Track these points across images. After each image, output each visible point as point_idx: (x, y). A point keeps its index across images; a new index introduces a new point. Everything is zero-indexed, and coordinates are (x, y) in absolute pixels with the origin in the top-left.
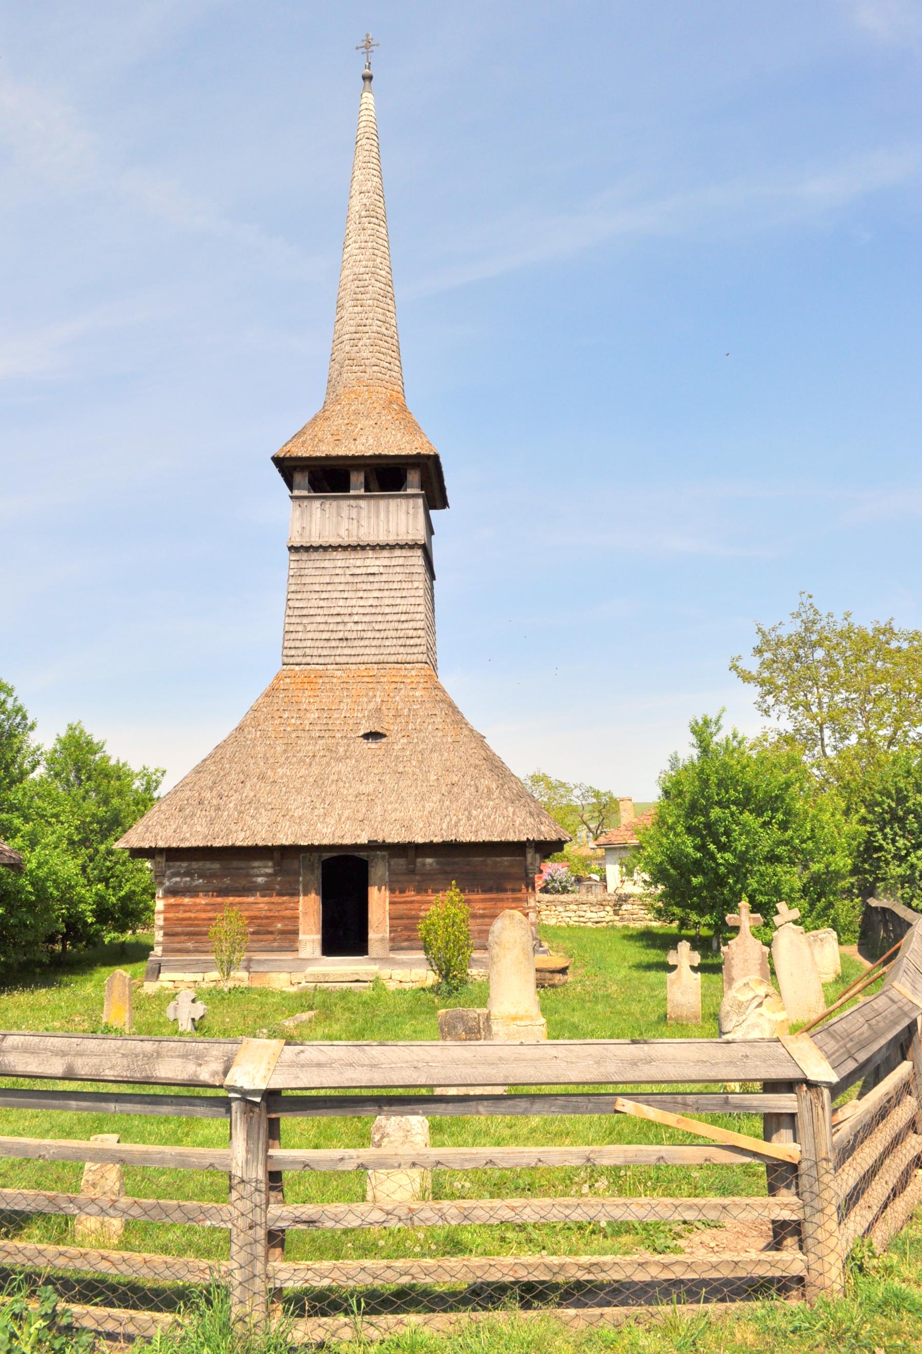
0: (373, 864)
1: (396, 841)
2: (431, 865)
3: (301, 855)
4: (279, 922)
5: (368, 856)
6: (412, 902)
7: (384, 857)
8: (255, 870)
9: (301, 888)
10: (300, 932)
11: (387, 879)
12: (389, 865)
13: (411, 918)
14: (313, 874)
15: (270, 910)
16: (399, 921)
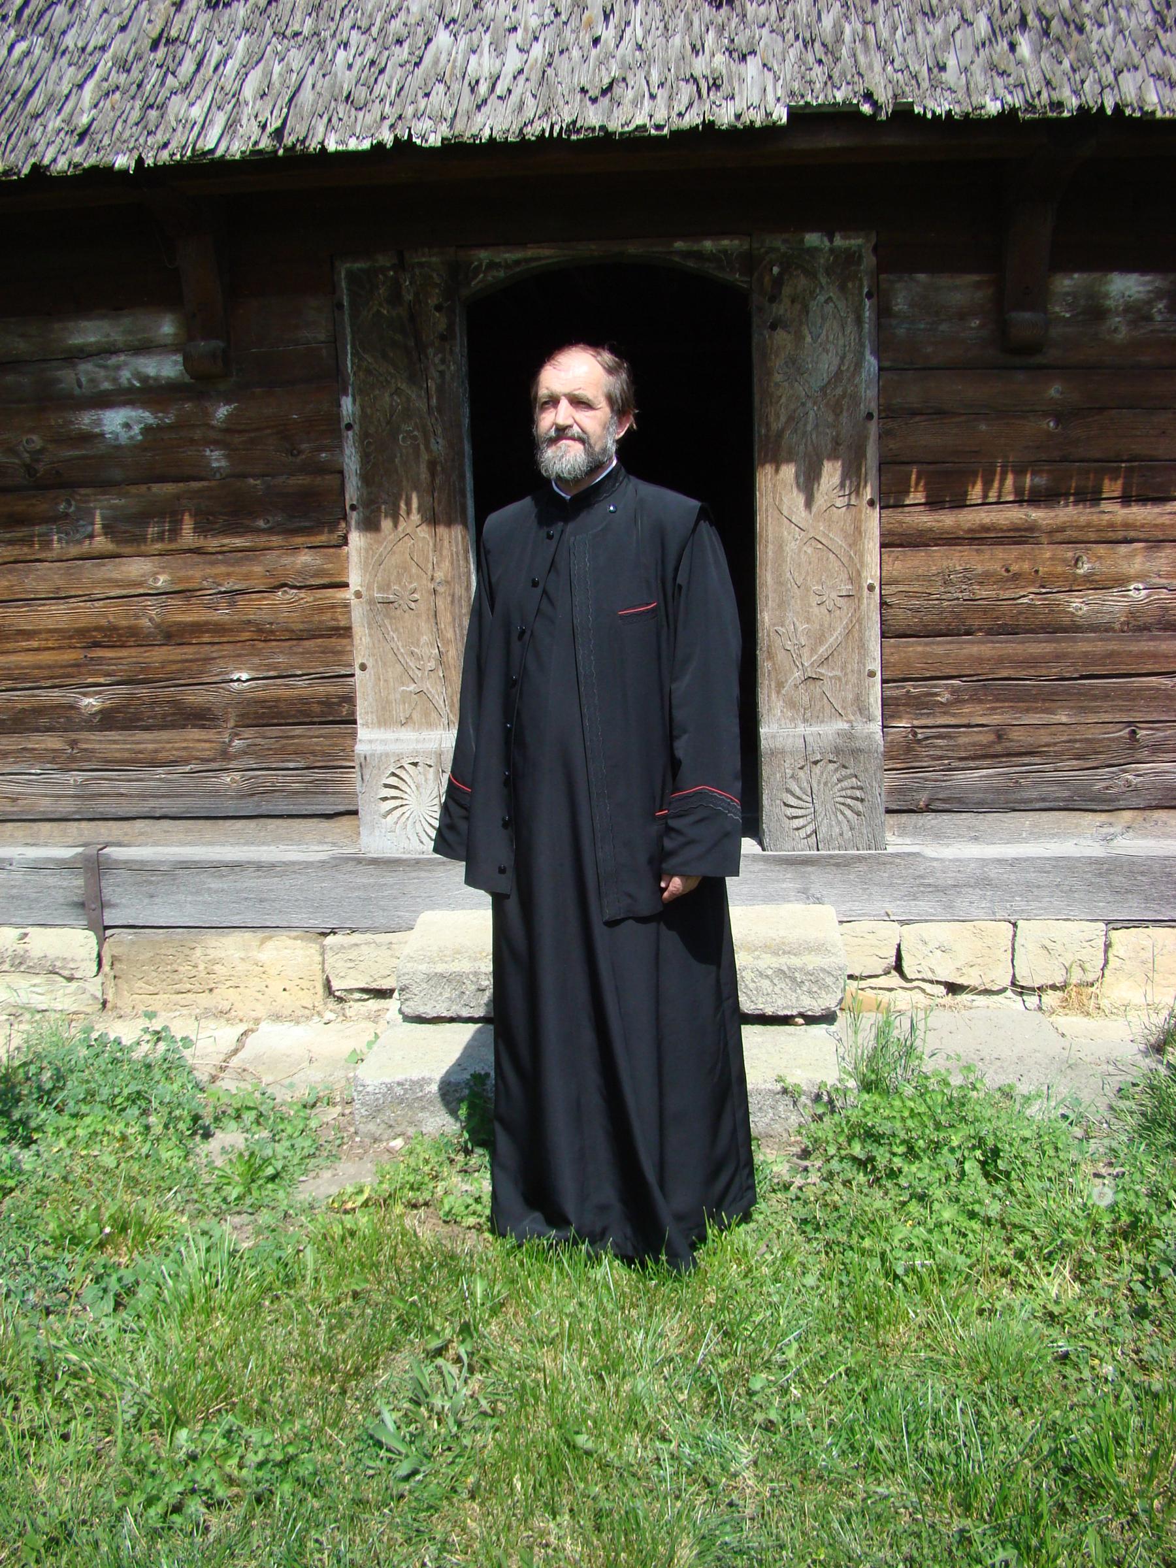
0: (782, 309)
1: (993, 108)
2: (1137, 313)
3: (343, 269)
4: (239, 659)
5: (750, 262)
6: (1020, 536)
7: (850, 259)
8: (86, 369)
9: (351, 461)
10: (363, 709)
11: (869, 396)
12: (883, 312)
13: (1011, 630)
14: (415, 377)
15: (185, 593)
16: (939, 647)
